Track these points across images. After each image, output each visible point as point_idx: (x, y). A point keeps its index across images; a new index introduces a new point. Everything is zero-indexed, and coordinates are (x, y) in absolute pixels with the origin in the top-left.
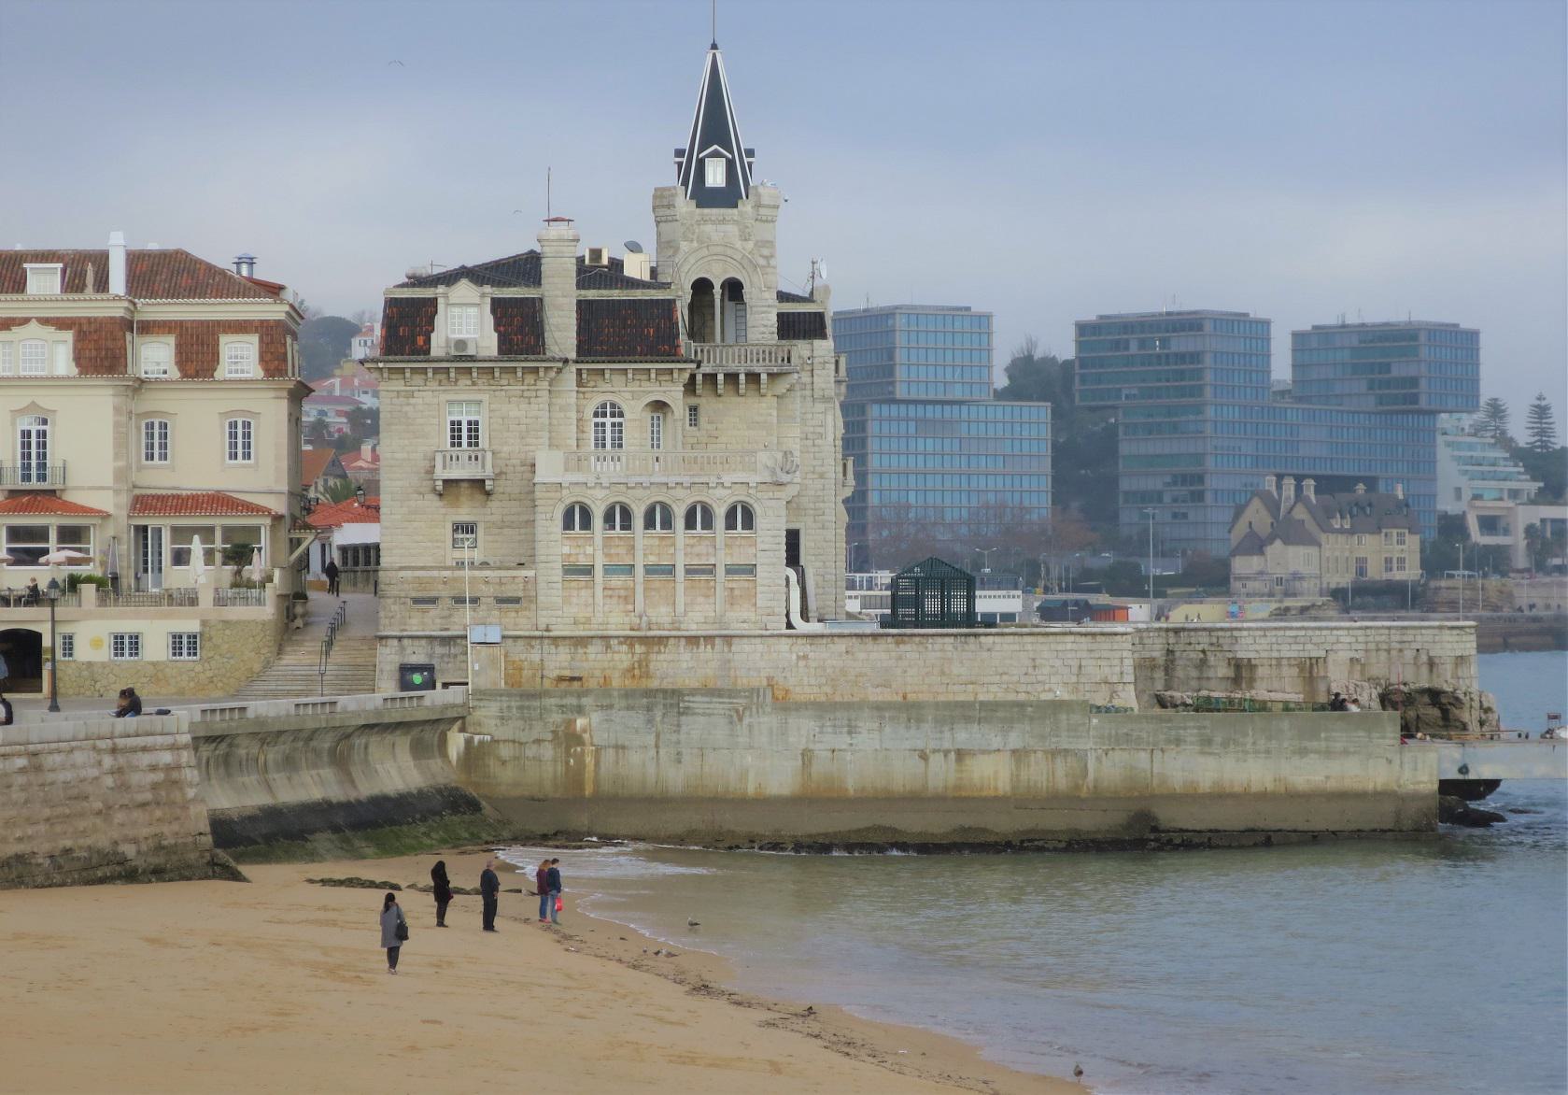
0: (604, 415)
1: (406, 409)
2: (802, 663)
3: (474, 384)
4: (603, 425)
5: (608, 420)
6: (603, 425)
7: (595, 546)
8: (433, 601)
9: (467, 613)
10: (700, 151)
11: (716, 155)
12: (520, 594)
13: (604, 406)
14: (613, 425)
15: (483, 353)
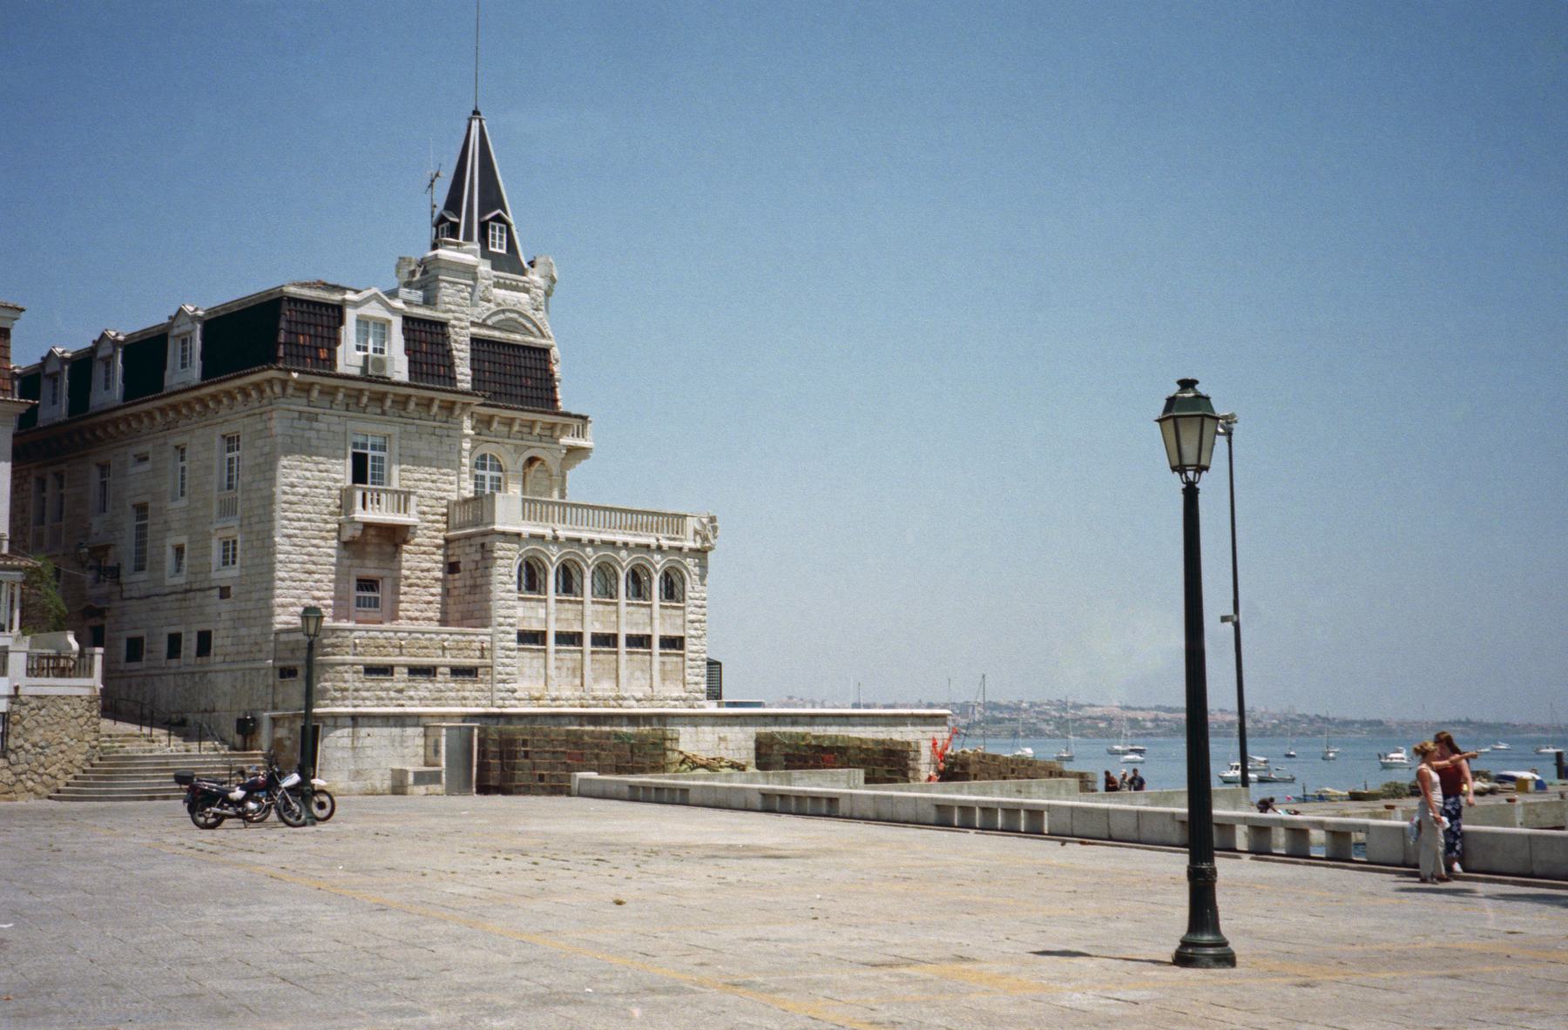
0: (484, 467)
1: (308, 434)
2: (723, 745)
3: (384, 413)
4: (483, 477)
5: (488, 474)
6: (483, 477)
7: (548, 614)
8: (386, 670)
9: (424, 687)
10: (481, 214)
11: (498, 219)
12: (476, 662)
13: (483, 457)
14: (492, 478)
15: (396, 378)
